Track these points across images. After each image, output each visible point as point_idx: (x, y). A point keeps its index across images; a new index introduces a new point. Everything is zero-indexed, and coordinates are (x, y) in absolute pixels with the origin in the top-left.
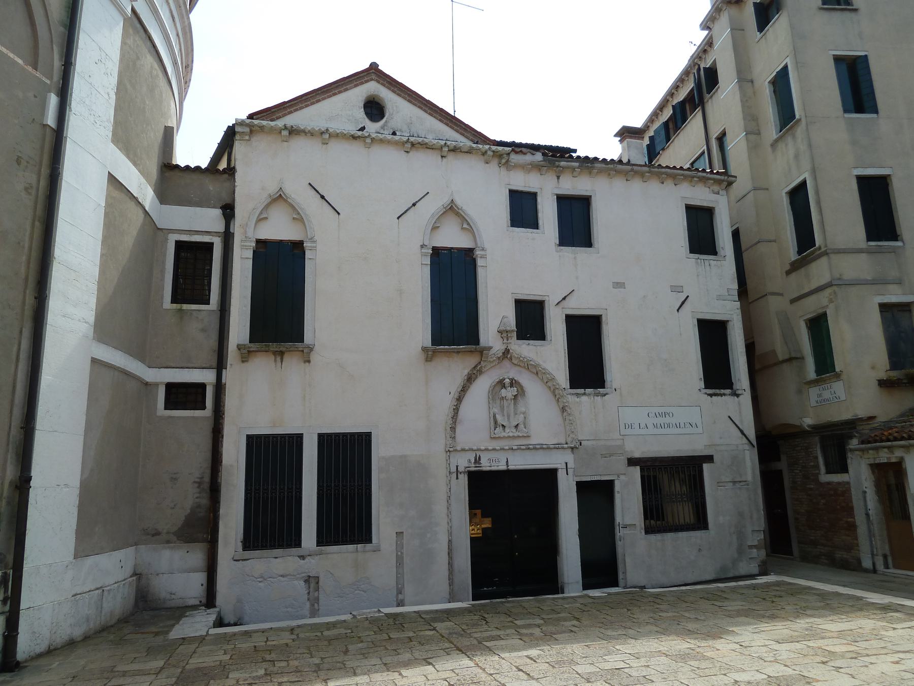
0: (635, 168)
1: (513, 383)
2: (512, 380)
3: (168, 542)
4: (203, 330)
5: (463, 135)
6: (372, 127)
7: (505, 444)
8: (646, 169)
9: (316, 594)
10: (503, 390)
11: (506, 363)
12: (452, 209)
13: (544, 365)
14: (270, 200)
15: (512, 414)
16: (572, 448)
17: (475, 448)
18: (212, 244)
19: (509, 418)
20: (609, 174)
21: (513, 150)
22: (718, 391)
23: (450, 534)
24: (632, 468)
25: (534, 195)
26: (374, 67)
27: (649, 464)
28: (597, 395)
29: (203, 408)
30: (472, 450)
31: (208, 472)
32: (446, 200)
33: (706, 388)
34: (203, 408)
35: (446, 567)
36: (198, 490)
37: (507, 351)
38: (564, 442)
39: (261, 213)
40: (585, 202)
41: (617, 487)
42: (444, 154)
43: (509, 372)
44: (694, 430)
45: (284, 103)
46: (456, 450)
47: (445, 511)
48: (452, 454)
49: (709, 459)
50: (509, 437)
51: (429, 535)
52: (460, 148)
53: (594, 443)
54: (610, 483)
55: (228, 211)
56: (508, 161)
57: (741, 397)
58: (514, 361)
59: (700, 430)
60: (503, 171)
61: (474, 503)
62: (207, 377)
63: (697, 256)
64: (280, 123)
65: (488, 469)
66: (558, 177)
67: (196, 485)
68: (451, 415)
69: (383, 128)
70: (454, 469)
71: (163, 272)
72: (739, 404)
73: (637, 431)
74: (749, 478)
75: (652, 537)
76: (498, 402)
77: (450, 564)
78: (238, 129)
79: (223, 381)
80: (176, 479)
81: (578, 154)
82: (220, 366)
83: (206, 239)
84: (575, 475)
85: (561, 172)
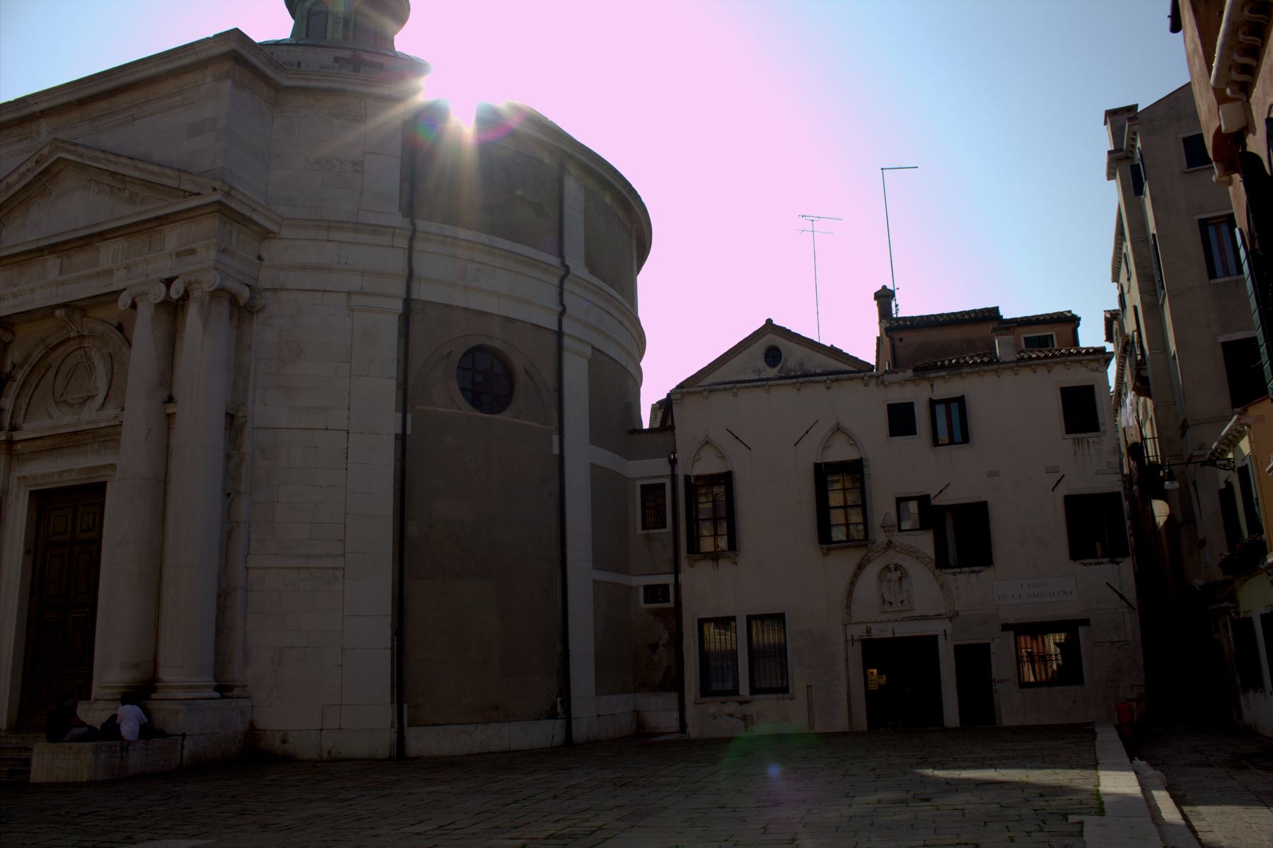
1: (897, 567)
6: (772, 372)
11: (891, 551)
12: (838, 429)
23: (848, 686)
28: (973, 572)
37: (890, 543)
40: (961, 401)
41: (993, 649)
43: (894, 558)
49: (1086, 622)
54: (987, 646)
61: (867, 665)
62: (669, 579)
63: (1074, 435)
77: (850, 709)
82: (677, 572)
83: (660, 481)
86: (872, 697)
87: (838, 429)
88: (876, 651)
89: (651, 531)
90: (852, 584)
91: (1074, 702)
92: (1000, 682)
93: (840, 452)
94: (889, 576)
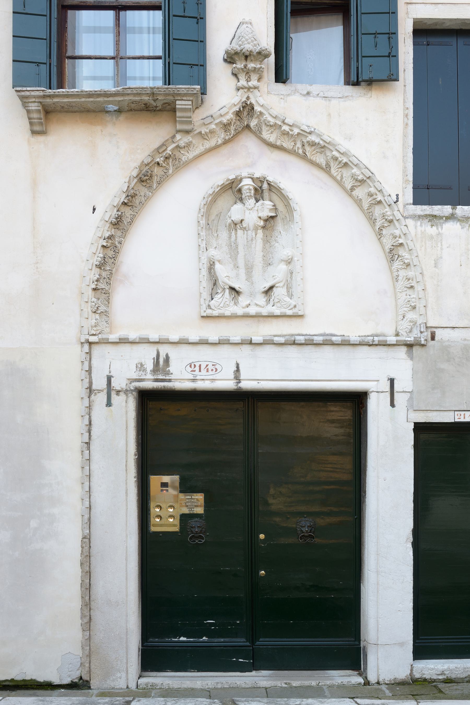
1: (262, 189)
2: (261, 180)
7: (236, 331)
10: (239, 206)
11: (248, 143)
16: (410, 346)
17: (154, 337)
19: (249, 269)
30: (145, 341)
46: (107, 342)
48: (96, 350)
50: (246, 316)
70: (100, 383)
76: (224, 234)
94: (237, 212)
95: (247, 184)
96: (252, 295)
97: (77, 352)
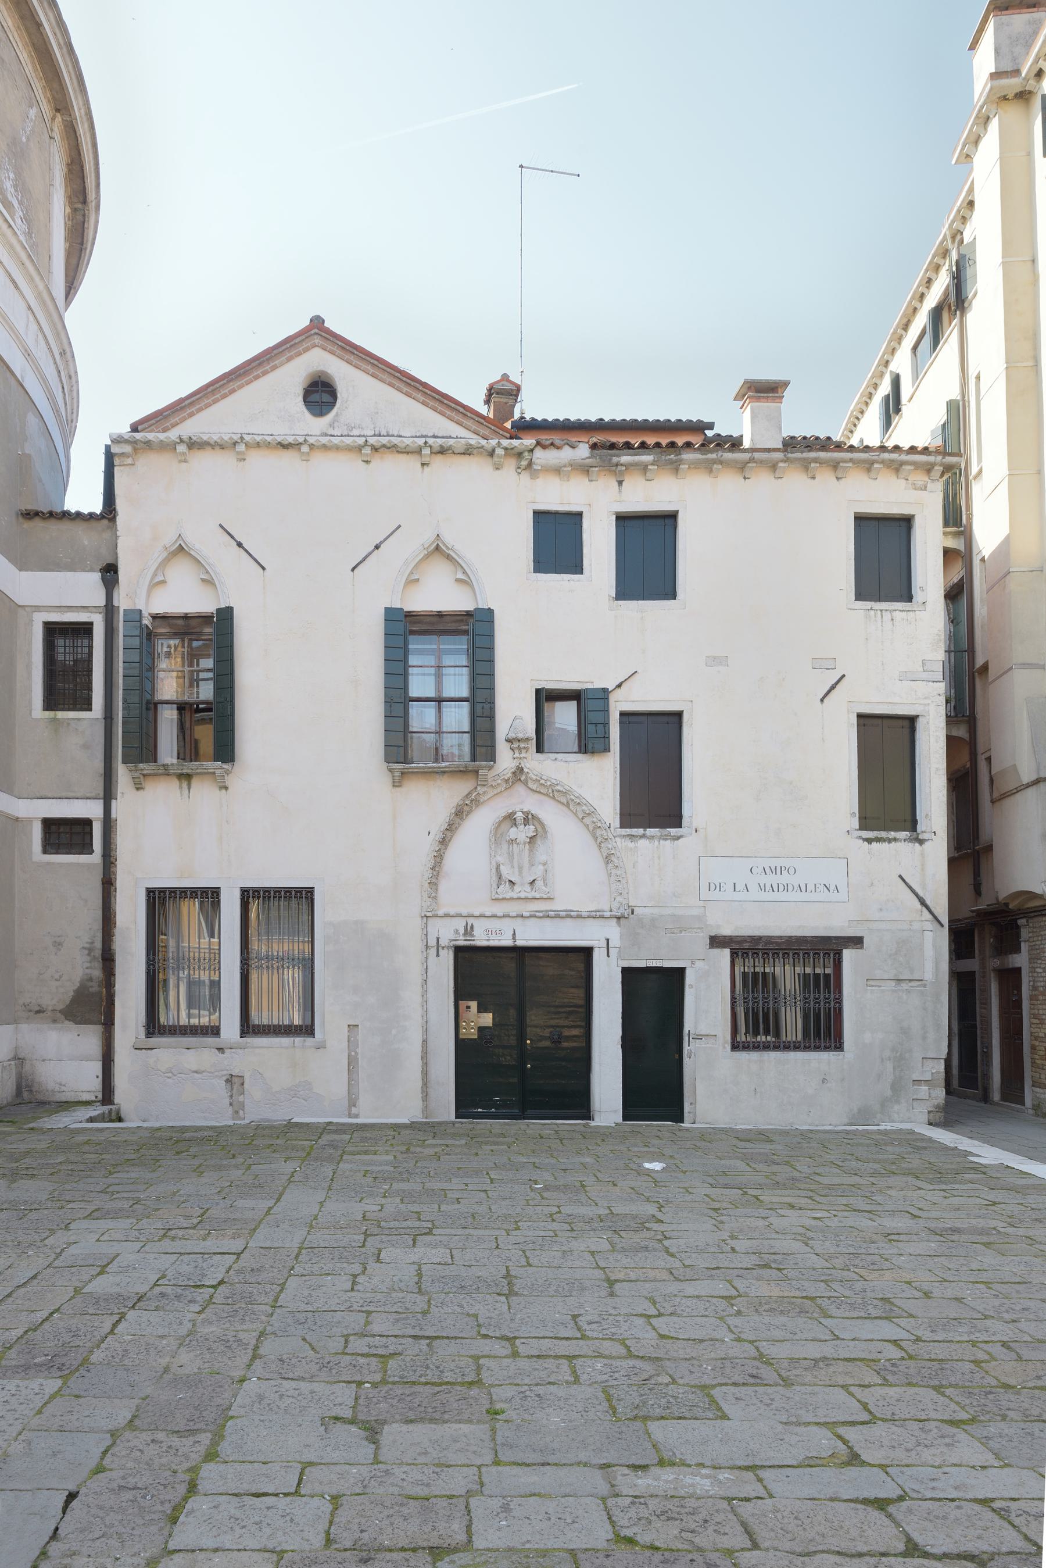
0: (757, 455)
1: (529, 818)
3: (55, 1021)
4: (86, 746)
5: (460, 424)
7: (513, 908)
8: (779, 455)
9: (241, 1098)
10: (514, 829)
11: (520, 788)
12: (438, 550)
13: (578, 791)
14: (165, 554)
15: (526, 864)
16: (619, 918)
17: (465, 912)
18: (91, 624)
19: (520, 869)
20: (711, 471)
21: (538, 443)
22: (883, 834)
23: (426, 1031)
24: (716, 951)
25: (577, 517)
26: (317, 324)
27: (746, 946)
29: (91, 852)
30: (460, 916)
31: (99, 935)
32: (427, 538)
33: (862, 828)
34: (91, 852)
35: (418, 1075)
36: (89, 958)
37: (520, 770)
38: (607, 908)
39: (155, 575)
41: (690, 978)
42: (426, 460)
43: (522, 801)
44: (833, 896)
45: (181, 400)
46: (437, 916)
47: (419, 999)
48: (431, 921)
49: (857, 942)
50: (519, 899)
51: (394, 1032)
52: (450, 448)
53: (656, 911)
54: (681, 972)
55: (110, 572)
56: (530, 464)
57: (927, 845)
58: (530, 785)
59: (843, 896)
60: (525, 476)
61: (461, 993)
62: (92, 810)
63: (868, 604)
64: (173, 435)
65: (484, 943)
66: (620, 483)
67: (87, 952)
68: (431, 864)
69: (331, 425)
70: (432, 942)
71: (29, 667)
72: (922, 855)
73: (728, 894)
74: (929, 975)
75: (744, 1056)
76: (505, 846)
77: (425, 1073)
78: (115, 449)
79: (113, 816)
80: (60, 944)
81: (716, 430)
82: (108, 796)
84: (620, 957)
85: (621, 473)
86: (466, 1052)
87: (438, 550)
88: (478, 970)
89: (60, 714)
90: (444, 842)
91: (824, 1080)
92: (699, 1037)
93: (439, 595)
94: (513, 832)
95: (519, 816)
96: (522, 884)
97: (419, 922)
